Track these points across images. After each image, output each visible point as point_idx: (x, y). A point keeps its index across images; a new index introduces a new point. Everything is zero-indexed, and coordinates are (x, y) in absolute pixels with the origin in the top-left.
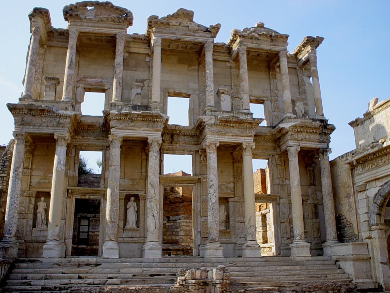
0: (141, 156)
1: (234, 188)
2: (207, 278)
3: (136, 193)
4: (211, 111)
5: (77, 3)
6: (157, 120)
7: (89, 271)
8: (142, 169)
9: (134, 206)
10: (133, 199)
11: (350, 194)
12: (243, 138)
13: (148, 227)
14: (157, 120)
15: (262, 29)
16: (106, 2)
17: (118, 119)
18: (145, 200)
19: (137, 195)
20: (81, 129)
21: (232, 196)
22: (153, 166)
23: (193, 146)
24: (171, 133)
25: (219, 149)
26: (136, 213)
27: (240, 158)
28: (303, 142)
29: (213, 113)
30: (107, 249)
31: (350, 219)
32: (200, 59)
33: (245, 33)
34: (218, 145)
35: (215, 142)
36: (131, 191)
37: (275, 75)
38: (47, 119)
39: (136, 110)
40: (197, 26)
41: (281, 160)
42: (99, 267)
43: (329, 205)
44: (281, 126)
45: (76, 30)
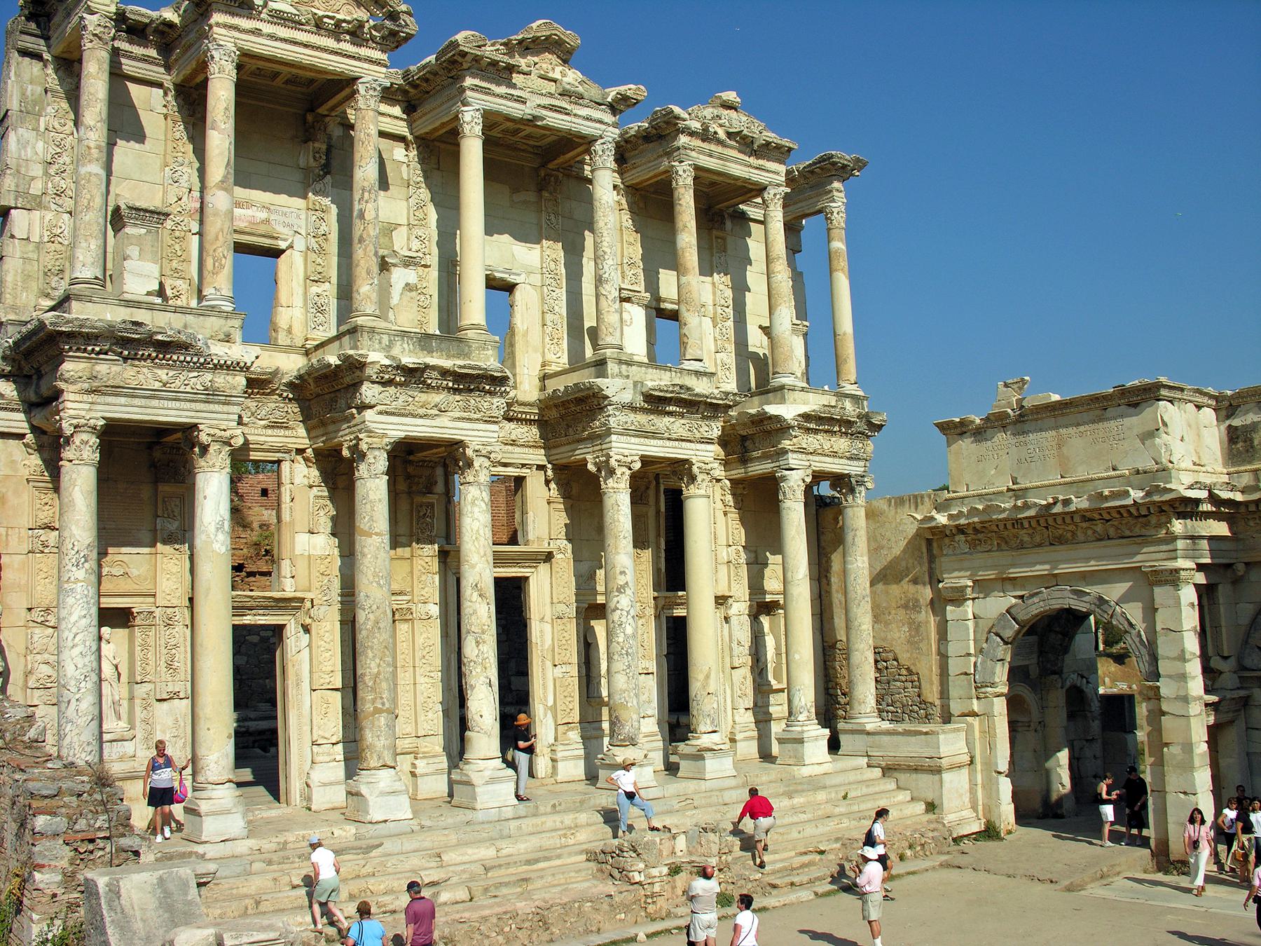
2: (673, 853)
7: (364, 871)
11: (917, 601)
13: (477, 717)
15: (733, 113)
22: (481, 532)
23: (531, 450)
25: (635, 479)
27: (643, 488)
28: (817, 458)
29: (624, 367)
30: (383, 794)
31: (914, 664)
33: (696, 125)
34: (637, 466)
35: (629, 459)
37: (724, 239)
38: (171, 373)
39: (430, 352)
41: (733, 495)
42: (374, 853)
43: (864, 627)
44: (772, 409)
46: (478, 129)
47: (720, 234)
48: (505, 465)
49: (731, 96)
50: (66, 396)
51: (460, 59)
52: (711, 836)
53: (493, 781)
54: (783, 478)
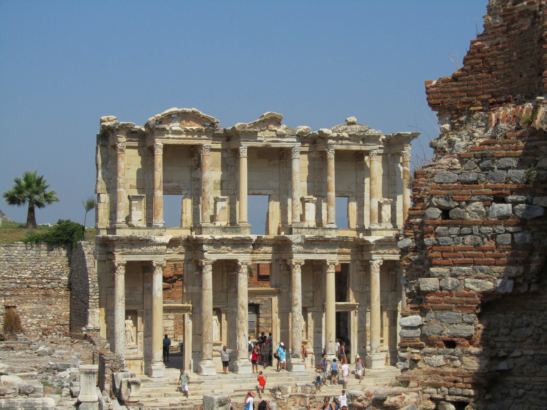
1: (313, 297)
2: (296, 392)
3: (218, 306)
4: (298, 228)
8: (223, 281)
12: (327, 255)
15: (353, 126)
21: (311, 305)
29: (299, 230)
33: (335, 135)
34: (303, 263)
39: (226, 232)
40: (285, 130)
42: (202, 384)
44: (367, 238)
45: (162, 143)
46: (245, 154)
47: (360, 163)
48: (264, 260)
49: (352, 119)
50: (116, 256)
52: (308, 388)
53: (244, 366)
54: (372, 264)
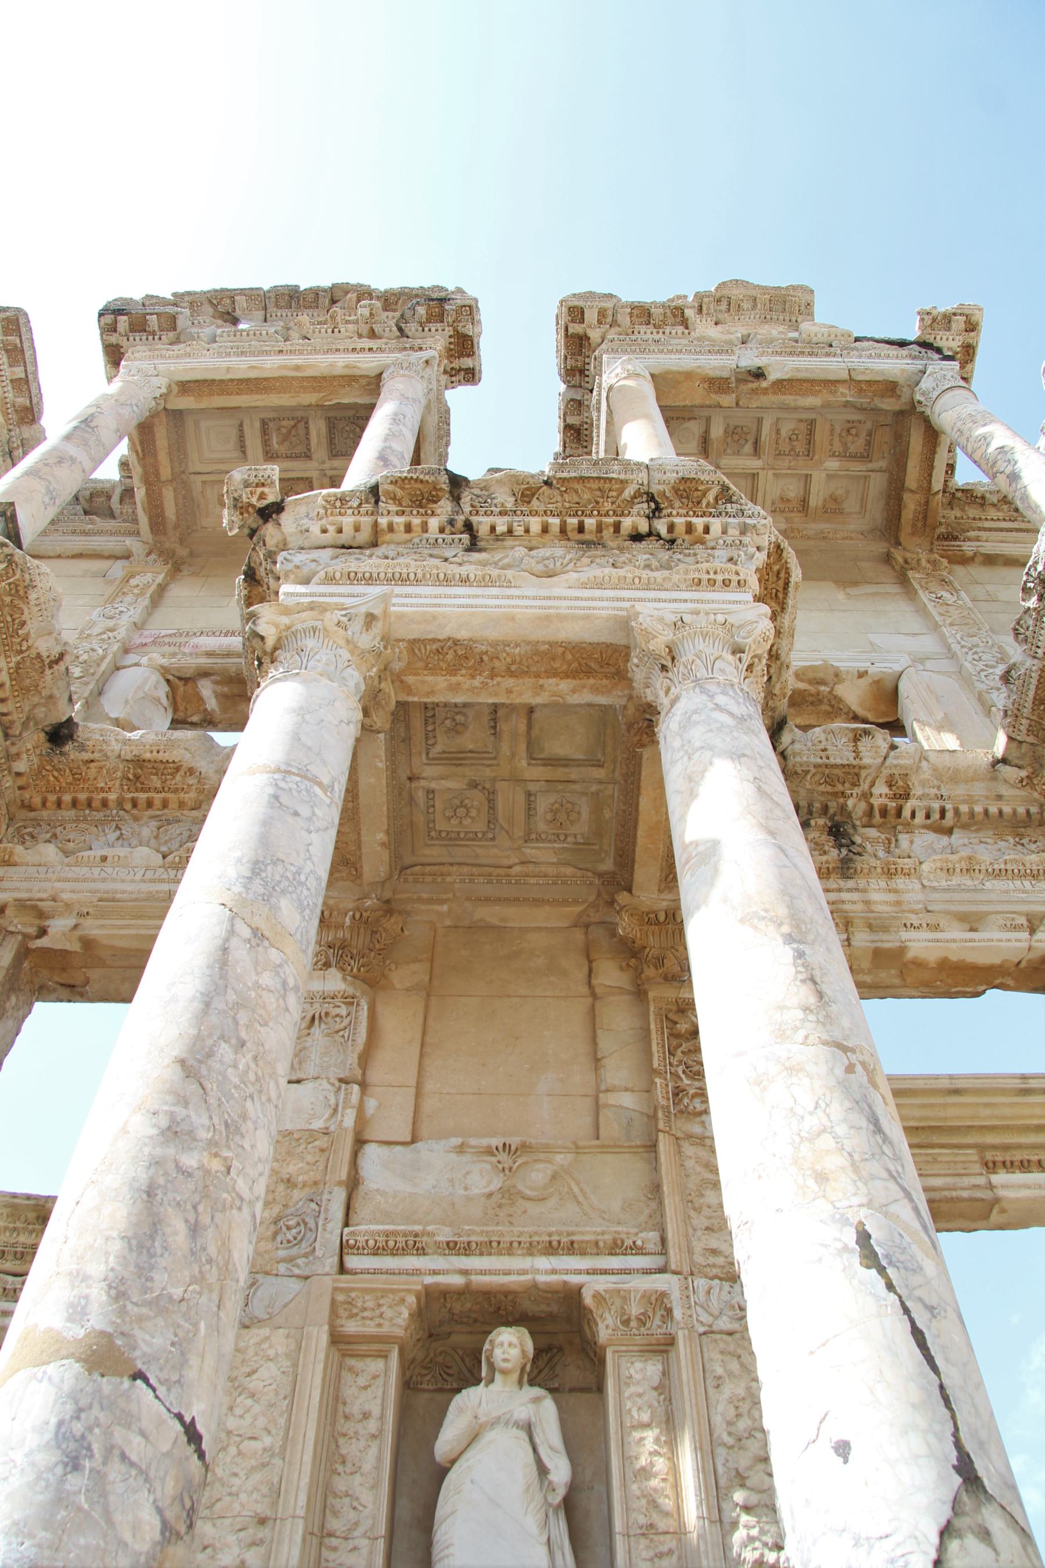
0: (581, 974)
5: (175, 295)
6: (699, 522)
8: (597, 1061)
9: (529, 1429)
10: (509, 1345)
14: (699, 522)
16: (334, 286)
17: (345, 538)
18: (665, 1347)
19: (571, 1297)
20: (75, 803)
24: (825, 809)
26: (560, 1529)
32: (898, 555)
36: (486, 1248)
51: (576, 328)
